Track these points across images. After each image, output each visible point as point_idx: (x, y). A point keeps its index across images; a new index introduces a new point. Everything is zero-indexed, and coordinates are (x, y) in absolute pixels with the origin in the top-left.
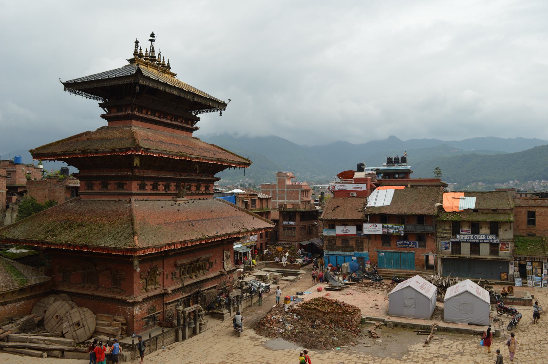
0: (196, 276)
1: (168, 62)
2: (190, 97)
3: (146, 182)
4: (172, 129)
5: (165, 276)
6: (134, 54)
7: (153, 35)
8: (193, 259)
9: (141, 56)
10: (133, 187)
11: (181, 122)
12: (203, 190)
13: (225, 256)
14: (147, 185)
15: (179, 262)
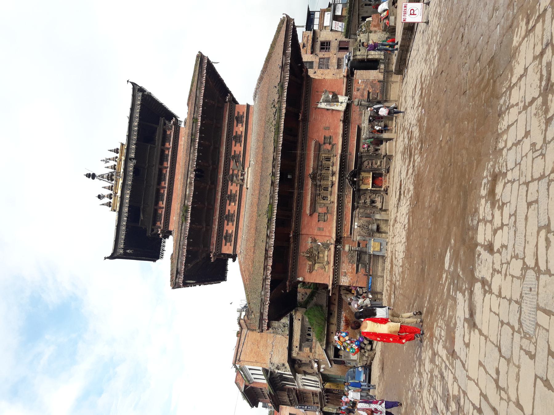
0: (333, 174)
1: (111, 151)
2: (131, 164)
3: (225, 232)
4: (177, 165)
5: (319, 233)
6: (110, 206)
7: (88, 176)
8: (310, 182)
9: (110, 196)
10: (227, 252)
11: (168, 149)
12: (241, 129)
13: (323, 105)
14: (227, 231)
15: (308, 212)
